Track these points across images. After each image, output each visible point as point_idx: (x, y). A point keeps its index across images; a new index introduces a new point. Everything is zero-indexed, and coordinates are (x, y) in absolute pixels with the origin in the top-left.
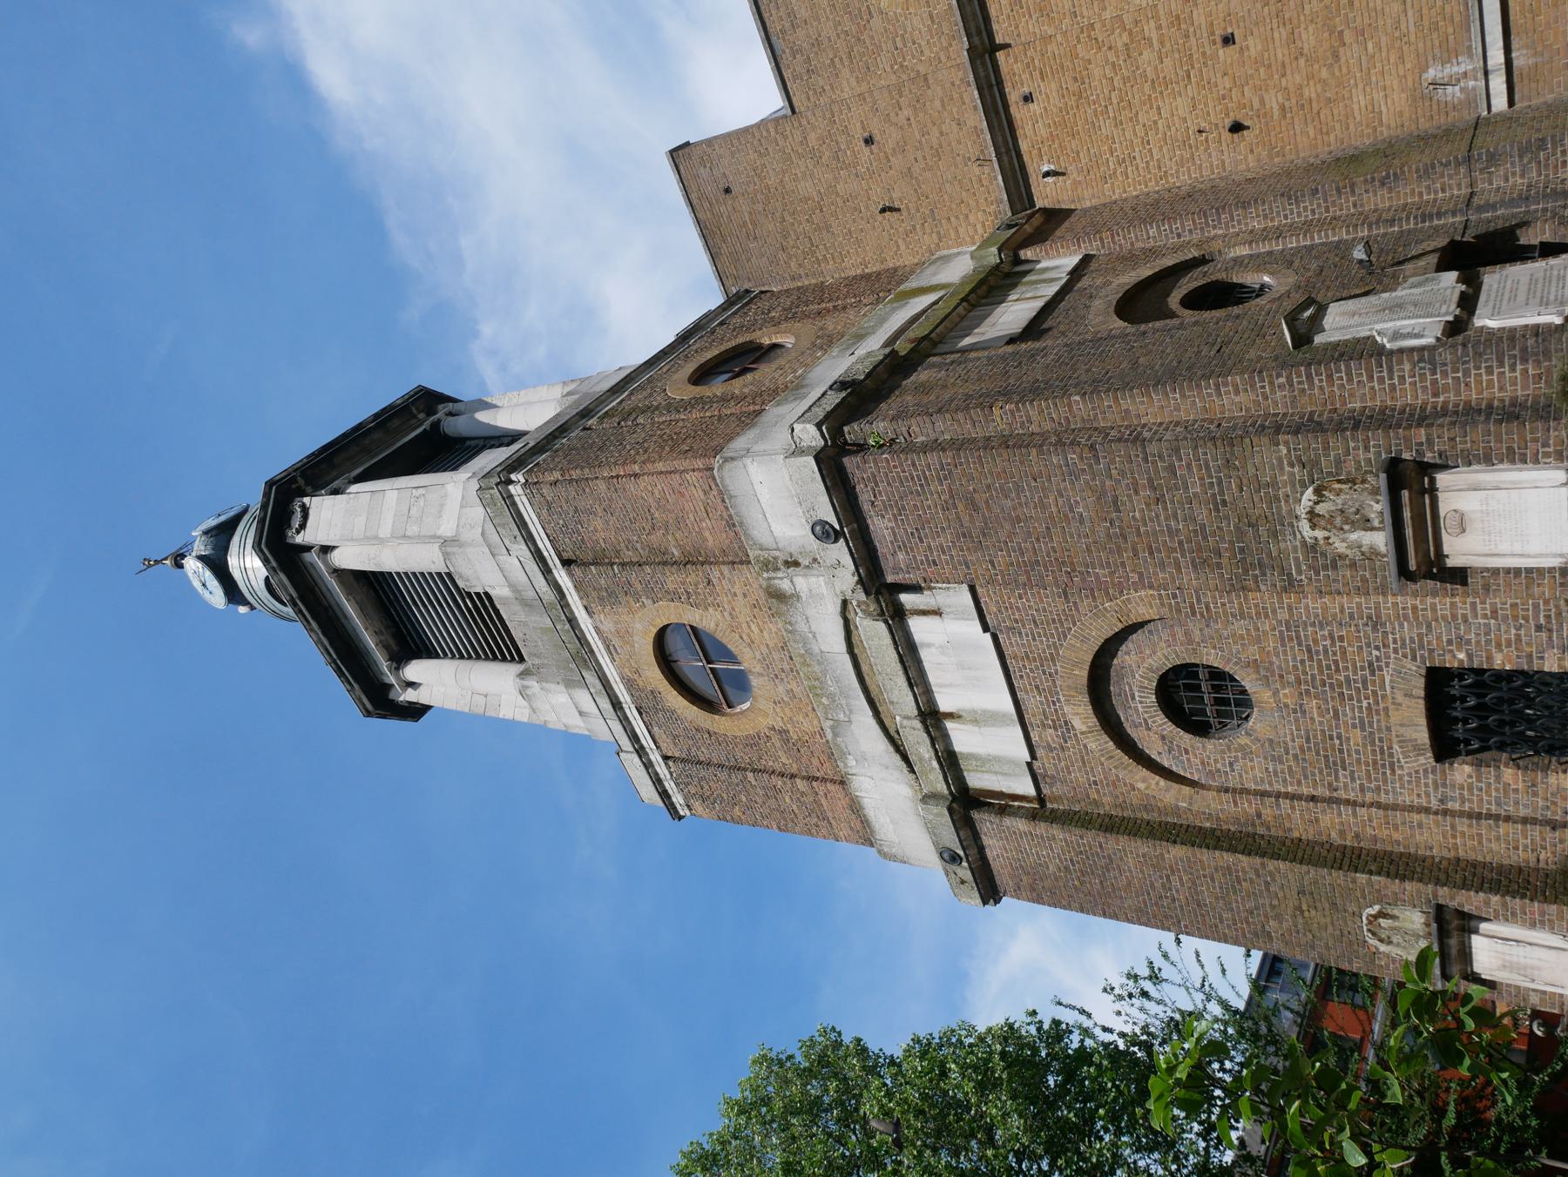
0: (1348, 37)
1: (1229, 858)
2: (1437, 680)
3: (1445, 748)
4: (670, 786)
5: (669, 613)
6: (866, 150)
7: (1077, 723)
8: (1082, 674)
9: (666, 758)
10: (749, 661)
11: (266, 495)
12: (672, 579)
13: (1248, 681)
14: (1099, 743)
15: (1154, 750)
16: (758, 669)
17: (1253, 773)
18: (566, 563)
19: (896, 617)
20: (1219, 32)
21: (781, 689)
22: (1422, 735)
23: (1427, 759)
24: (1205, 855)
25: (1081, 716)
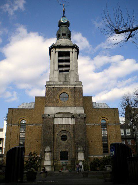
2: (67, 152)
3: (61, 152)
4: (50, 86)
7: (62, 129)
8: (66, 130)
11: (78, 47)
12: (73, 99)
14: (60, 130)
15: (60, 134)
17: (58, 140)
18: (75, 88)
22: (63, 151)
23: (61, 151)
24: (52, 136)
25: (63, 129)
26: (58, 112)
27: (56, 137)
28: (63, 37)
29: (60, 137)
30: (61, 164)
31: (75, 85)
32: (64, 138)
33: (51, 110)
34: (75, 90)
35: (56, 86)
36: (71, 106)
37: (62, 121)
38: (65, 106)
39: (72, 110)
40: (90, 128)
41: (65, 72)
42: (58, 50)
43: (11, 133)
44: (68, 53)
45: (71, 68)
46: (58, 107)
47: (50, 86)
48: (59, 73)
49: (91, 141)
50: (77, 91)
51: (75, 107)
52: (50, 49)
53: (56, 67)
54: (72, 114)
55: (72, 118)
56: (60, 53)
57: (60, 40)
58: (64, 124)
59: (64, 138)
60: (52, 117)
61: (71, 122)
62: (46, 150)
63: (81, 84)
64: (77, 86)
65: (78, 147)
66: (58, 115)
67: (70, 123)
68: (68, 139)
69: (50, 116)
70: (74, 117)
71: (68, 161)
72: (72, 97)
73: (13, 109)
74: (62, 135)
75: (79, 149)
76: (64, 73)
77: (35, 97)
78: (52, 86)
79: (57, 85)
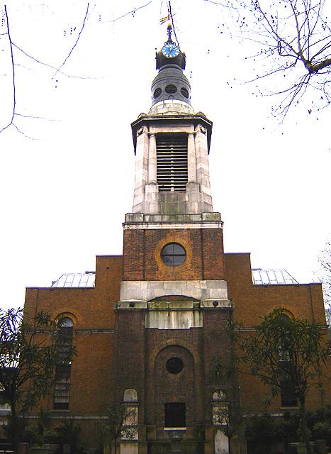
4: (134, 227)
8: (181, 344)
9: (144, 230)
11: (208, 121)
19: (193, 310)
23: (165, 402)
24: (143, 361)
26: (158, 295)
27: (152, 364)
28: (169, 95)
30: (167, 437)
31: (202, 222)
32: (174, 366)
33: (137, 291)
34: (202, 237)
35: (151, 227)
36: (191, 279)
37: (169, 321)
38: (178, 278)
39: (193, 289)
41: (175, 187)
42: (154, 130)
44: (183, 138)
45: (191, 176)
46: (158, 283)
47: (134, 227)
48: (160, 190)
50: (210, 239)
51: (205, 281)
52: (137, 127)
53: (153, 176)
54: (195, 300)
55: (197, 315)
56: (159, 137)
57: (162, 103)
59: (174, 366)
61: (194, 323)
62: (126, 398)
63: (217, 218)
64: (207, 226)
66: (160, 305)
68: (185, 369)
69: (136, 307)
70: (200, 310)
71: (185, 429)
72: (194, 256)
73: (38, 288)
75: (215, 396)
76: (172, 189)
77: (97, 256)
78: (140, 227)
79: (156, 223)
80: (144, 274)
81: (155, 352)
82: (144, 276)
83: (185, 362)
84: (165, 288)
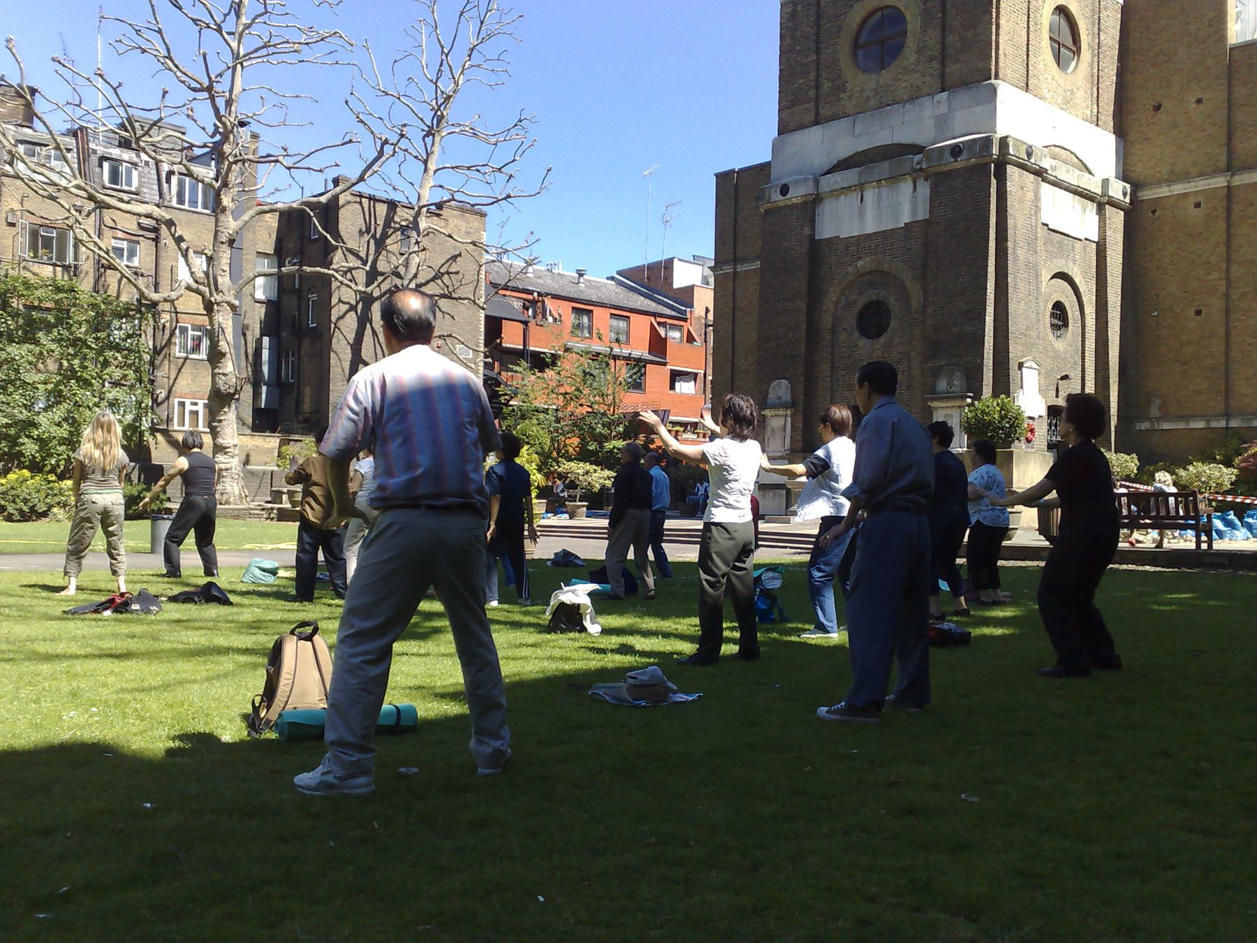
0: (1185, 367)
1: (804, 326)
5: (913, 23)
6: (1194, 100)
7: (860, 263)
10: (887, 76)
12: (933, 34)
13: (882, 339)
16: (882, 81)
17: (843, 337)
20: (1203, 309)
21: (871, 94)
24: (803, 317)
27: (827, 320)
29: (850, 318)
37: (862, 212)
40: (1192, 211)
43: (738, 313)
46: (844, 123)
49: (1198, 313)
58: (870, 229)
60: (805, 204)
61: (914, 209)
65: (936, 374)
66: (839, 179)
67: (905, 218)
68: (894, 324)
74: (862, 301)
75: (942, 385)
80: (817, 108)
81: (832, 295)
82: (817, 113)
83: (894, 304)
84: (857, 131)
